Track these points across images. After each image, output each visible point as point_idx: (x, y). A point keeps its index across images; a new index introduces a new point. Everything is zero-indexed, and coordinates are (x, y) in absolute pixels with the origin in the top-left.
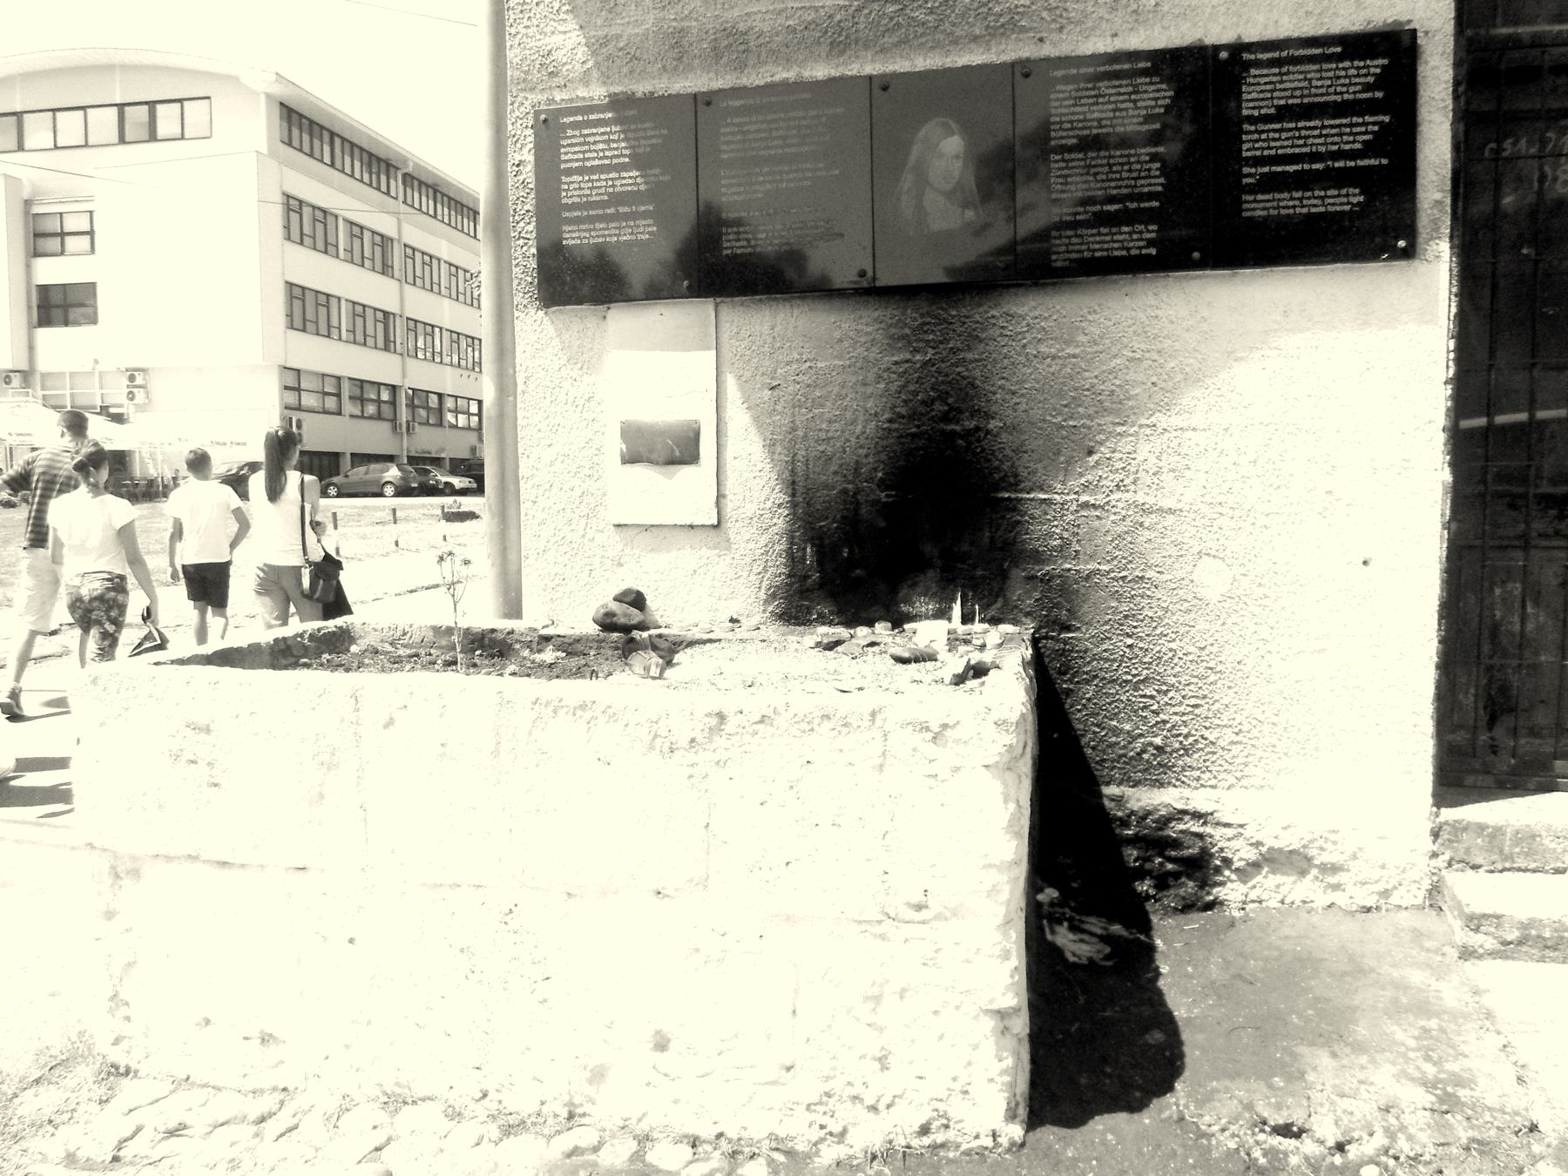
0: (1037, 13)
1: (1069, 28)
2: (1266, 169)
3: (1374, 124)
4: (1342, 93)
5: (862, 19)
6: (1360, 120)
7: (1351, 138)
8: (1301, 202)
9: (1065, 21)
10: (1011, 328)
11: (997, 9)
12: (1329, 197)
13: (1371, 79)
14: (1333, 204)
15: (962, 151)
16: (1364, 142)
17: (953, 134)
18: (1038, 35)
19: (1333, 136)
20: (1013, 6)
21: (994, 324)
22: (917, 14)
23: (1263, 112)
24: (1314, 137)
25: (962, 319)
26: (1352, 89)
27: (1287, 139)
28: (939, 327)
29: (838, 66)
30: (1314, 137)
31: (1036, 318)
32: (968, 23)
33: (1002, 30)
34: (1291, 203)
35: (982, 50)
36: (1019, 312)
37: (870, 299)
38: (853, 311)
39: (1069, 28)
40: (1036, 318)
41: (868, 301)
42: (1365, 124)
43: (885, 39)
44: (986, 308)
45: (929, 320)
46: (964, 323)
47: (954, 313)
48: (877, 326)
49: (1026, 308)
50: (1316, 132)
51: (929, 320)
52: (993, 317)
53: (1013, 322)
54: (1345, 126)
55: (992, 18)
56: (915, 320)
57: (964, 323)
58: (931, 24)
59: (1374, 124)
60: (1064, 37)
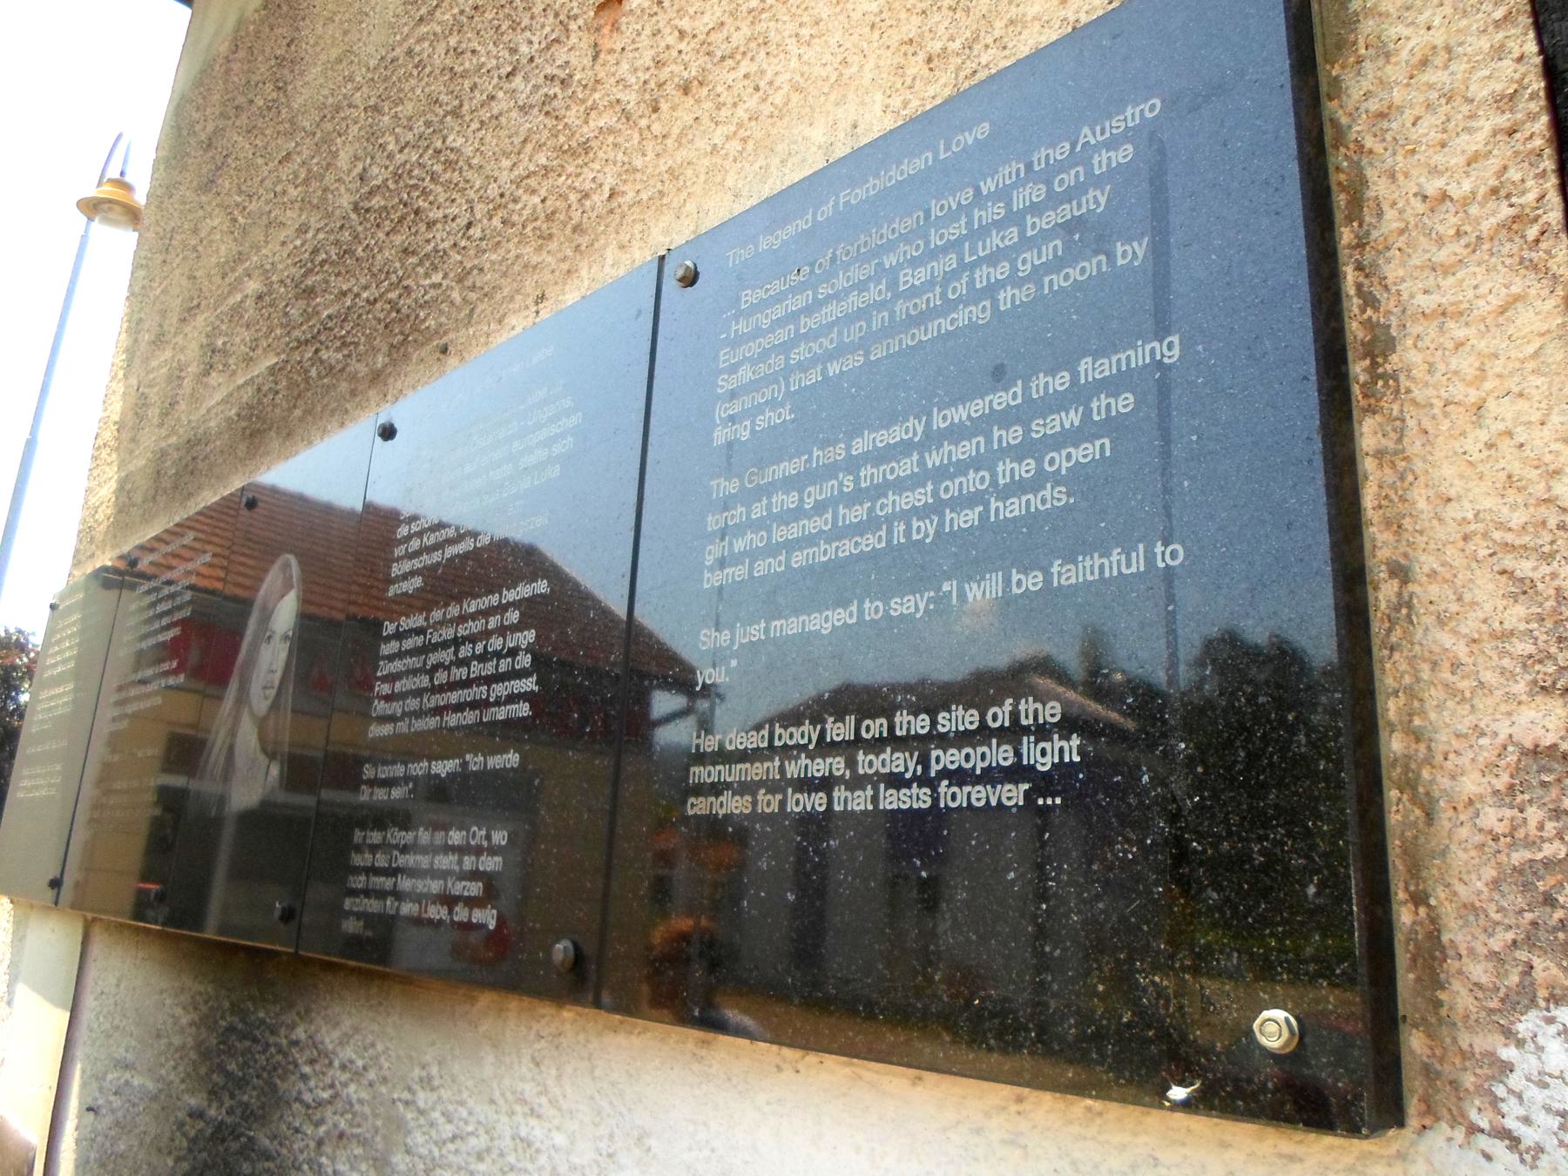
2: (756, 632)
3: (1112, 385)
4: (992, 290)
6: (1060, 382)
7: (1027, 468)
8: (851, 763)
12: (944, 741)
13: (1096, 200)
14: (960, 777)
16: (1077, 478)
19: (962, 468)
23: (762, 422)
24: (900, 486)
26: (1029, 260)
27: (820, 508)
30: (900, 486)
34: (819, 768)
42: (1079, 395)
50: (906, 467)
54: (1005, 418)
59: (1112, 385)
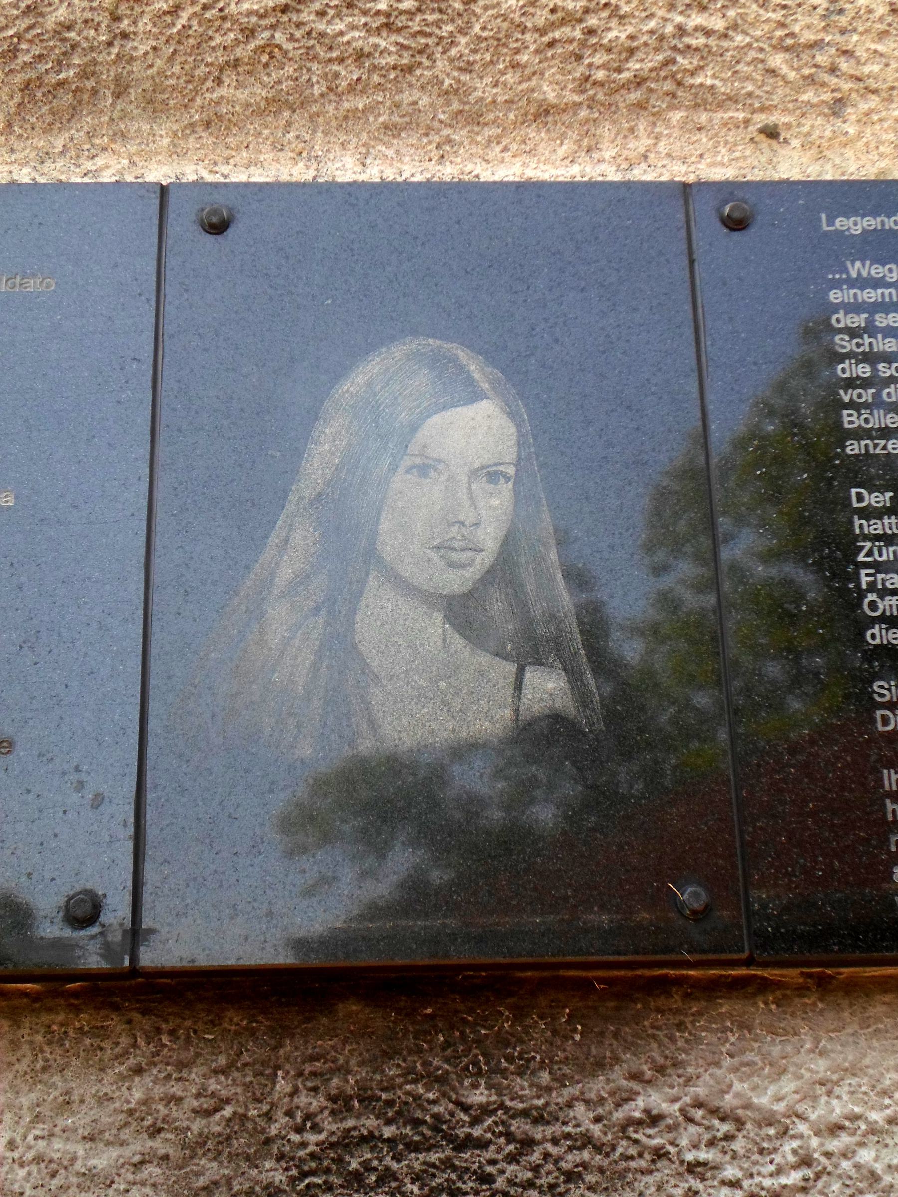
0: (752, 54)
1: (864, 106)
5: (145, 24)
9: (846, 86)
10: (731, 1172)
11: (617, 34)
15: (510, 455)
17: (476, 396)
18: (761, 119)
20: (669, 29)
21: (659, 1154)
22: (340, 26)
25: (516, 1126)
28: (416, 1161)
29: (45, 156)
31: (835, 1129)
32: (515, 66)
33: (635, 96)
35: (562, 151)
36: (763, 1100)
37: (114, 1022)
38: (35, 1077)
39: (864, 106)
40: (835, 1129)
41: (101, 1033)
43: (223, 91)
44: (618, 1077)
45: (370, 1122)
46: (528, 1143)
47: (479, 1097)
48: (138, 1146)
49: (788, 1085)
51: (370, 1122)
52: (653, 1119)
53: (739, 1145)
55: (599, 58)
56: (310, 1123)
57: (528, 1143)
58: (391, 60)
60: (851, 131)
